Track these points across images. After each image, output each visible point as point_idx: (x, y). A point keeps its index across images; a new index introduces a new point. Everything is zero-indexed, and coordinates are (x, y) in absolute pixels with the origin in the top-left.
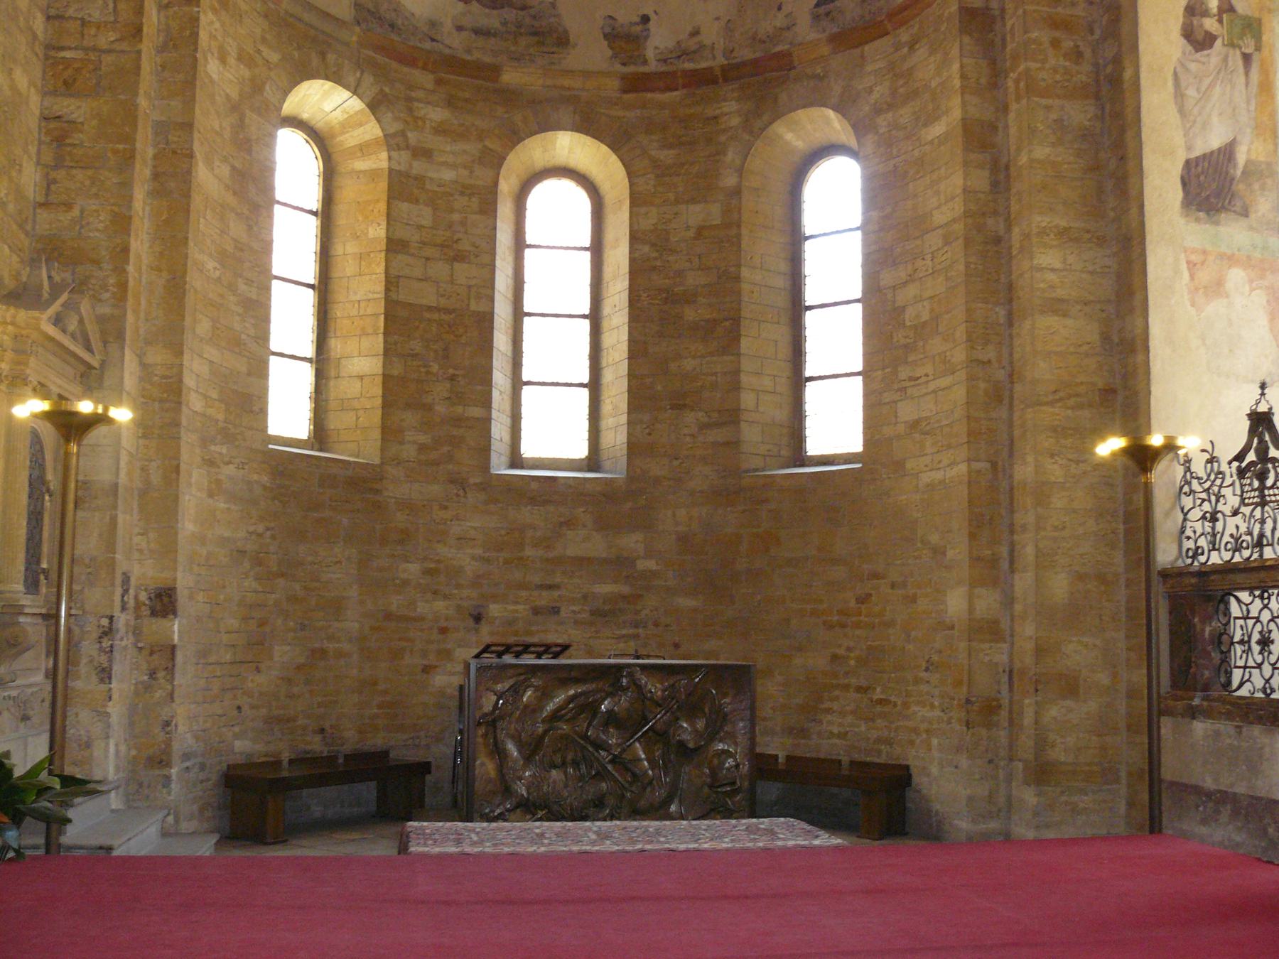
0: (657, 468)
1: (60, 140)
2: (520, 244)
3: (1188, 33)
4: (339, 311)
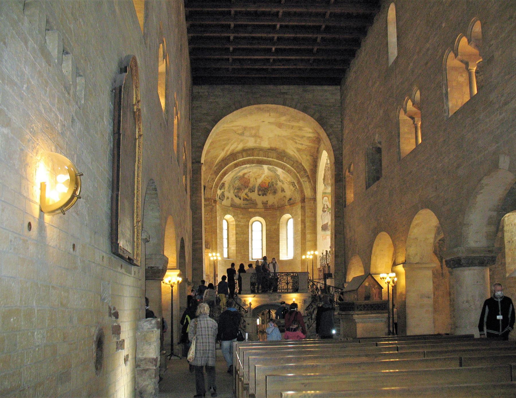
2: (252, 231)
4: (230, 242)
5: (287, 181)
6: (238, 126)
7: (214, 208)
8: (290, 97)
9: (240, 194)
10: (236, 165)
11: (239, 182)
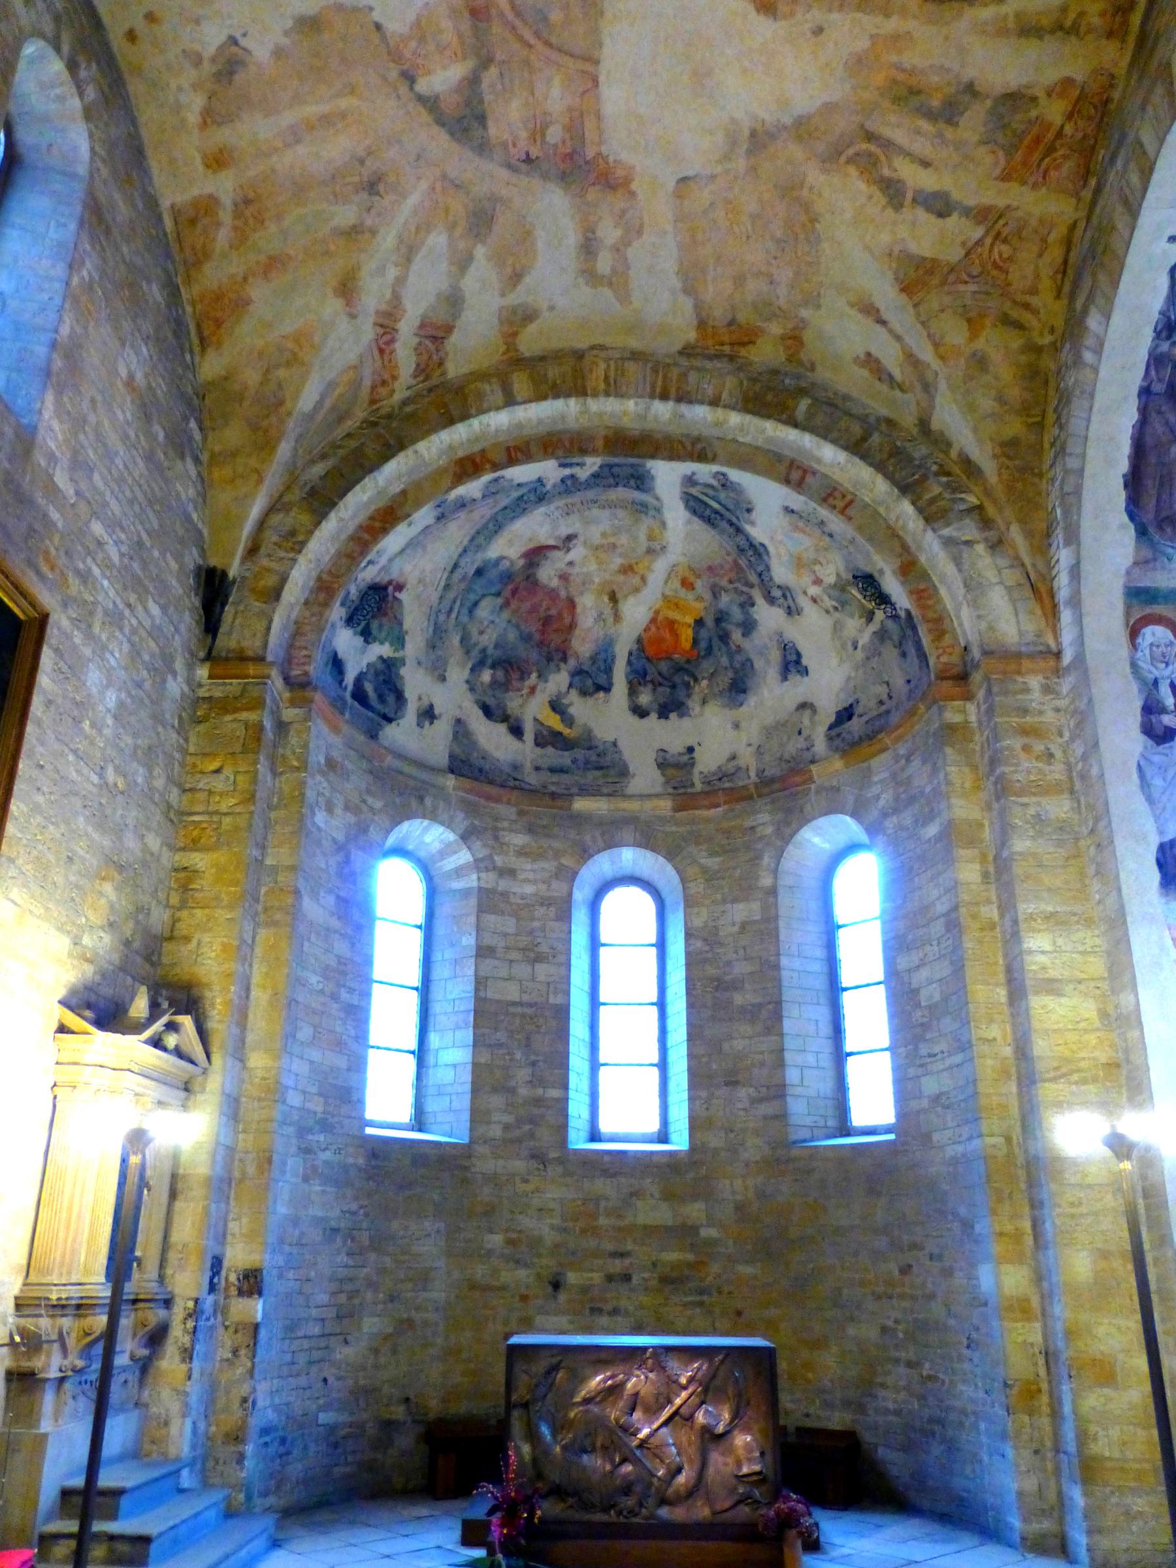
0: (715, 1140)
2: (595, 944)
3: (1148, 730)
4: (437, 1008)
5: (818, 582)
9: (513, 703)
11: (506, 615)
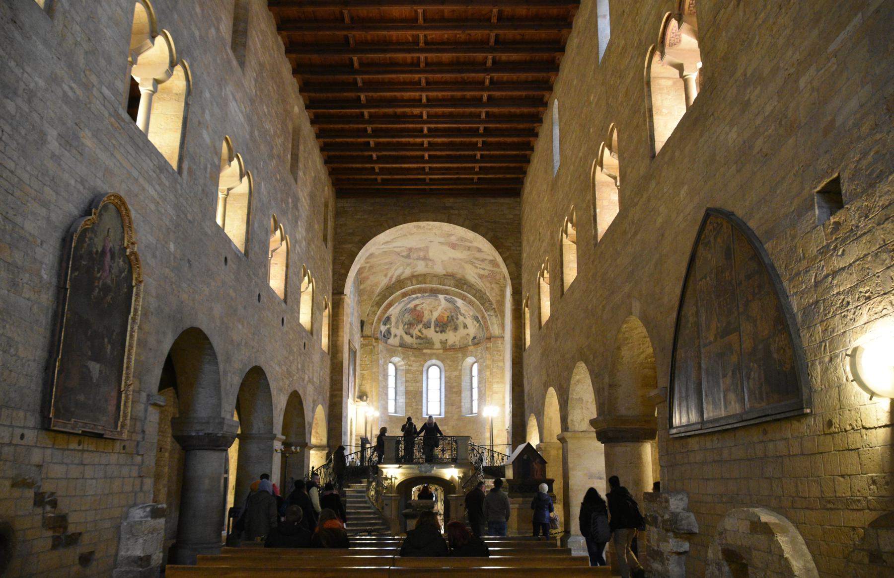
0: (449, 415)
1: (363, 377)
2: (427, 378)
4: (398, 392)
6: (400, 247)
7: (376, 349)
8: (456, 212)
9: (411, 331)
10: (404, 295)
